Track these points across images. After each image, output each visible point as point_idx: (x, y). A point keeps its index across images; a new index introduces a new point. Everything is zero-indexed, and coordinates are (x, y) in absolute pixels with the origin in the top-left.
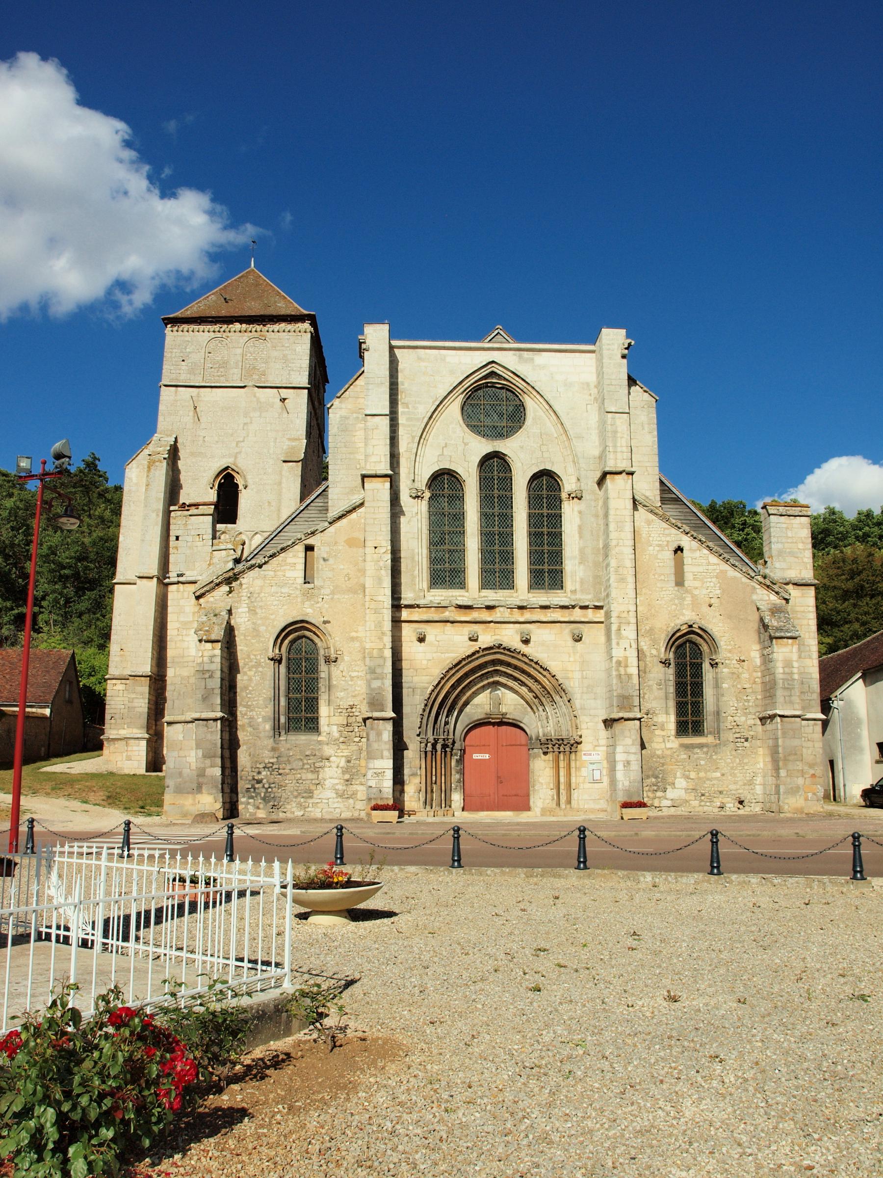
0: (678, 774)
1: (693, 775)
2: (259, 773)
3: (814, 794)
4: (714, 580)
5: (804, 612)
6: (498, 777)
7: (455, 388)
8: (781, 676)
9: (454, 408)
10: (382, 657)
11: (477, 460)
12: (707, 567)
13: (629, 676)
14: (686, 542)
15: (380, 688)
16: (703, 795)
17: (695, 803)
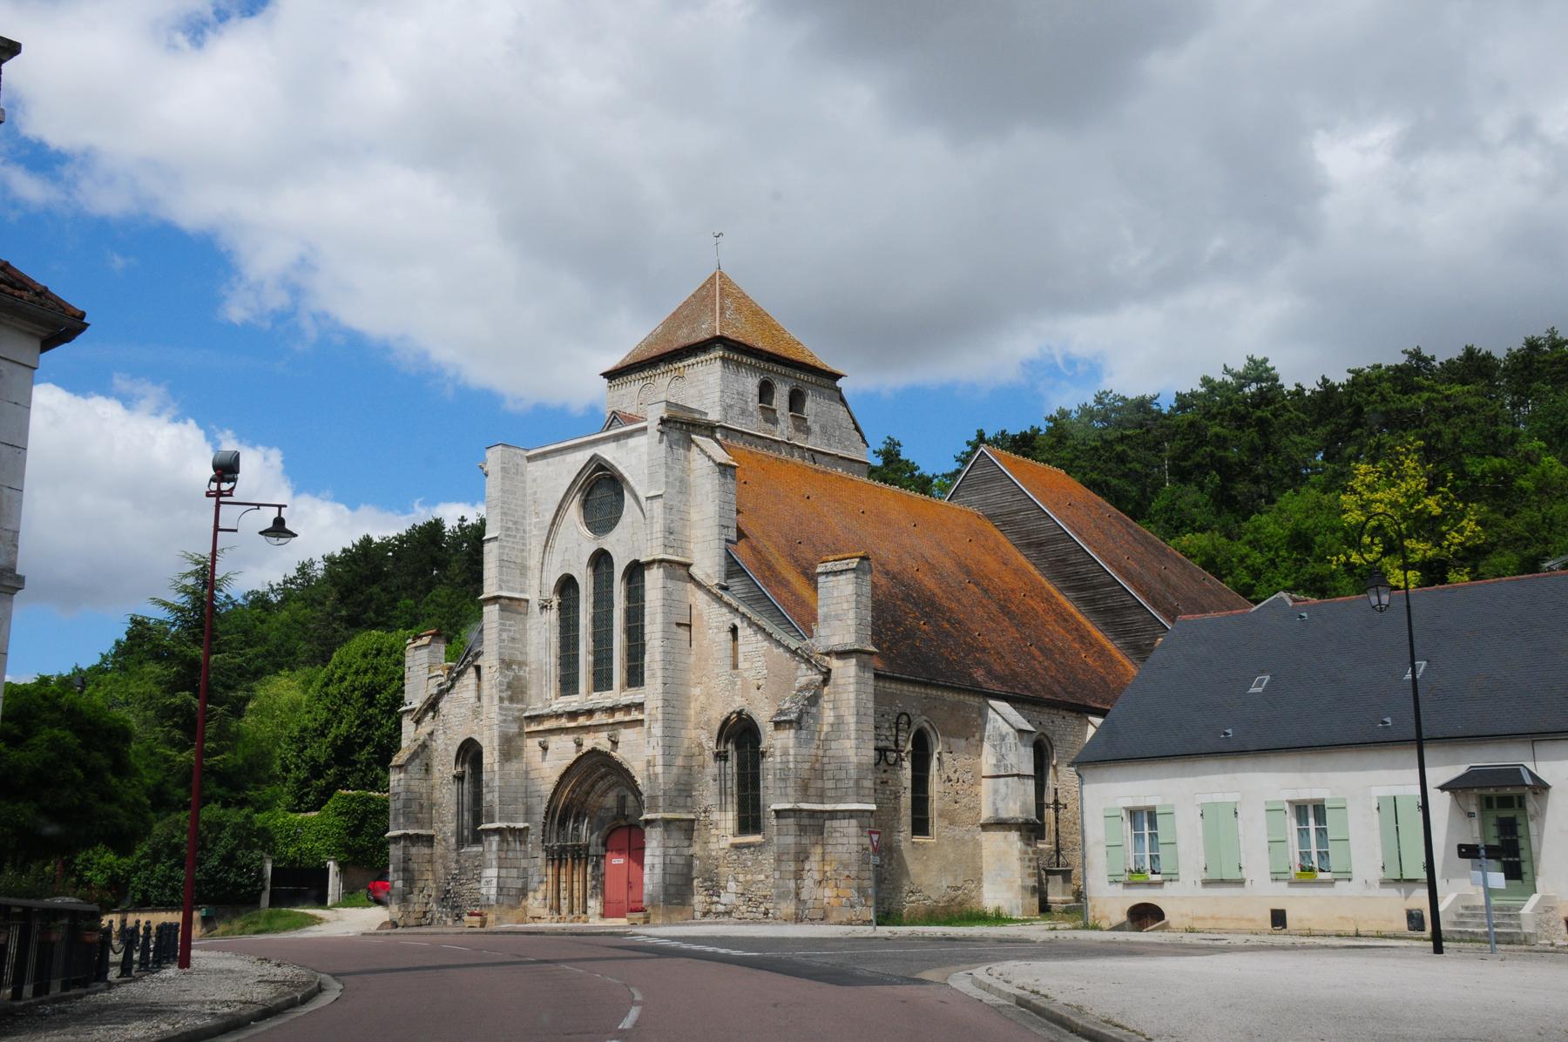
0: (730, 878)
1: (741, 878)
2: (449, 884)
3: (848, 899)
4: (762, 658)
5: (844, 685)
6: (629, 883)
7: (569, 489)
8: (778, 766)
9: (574, 512)
10: (493, 771)
11: (586, 559)
12: (755, 645)
13: (656, 775)
14: (738, 622)
15: (491, 801)
16: (750, 900)
17: (743, 908)
